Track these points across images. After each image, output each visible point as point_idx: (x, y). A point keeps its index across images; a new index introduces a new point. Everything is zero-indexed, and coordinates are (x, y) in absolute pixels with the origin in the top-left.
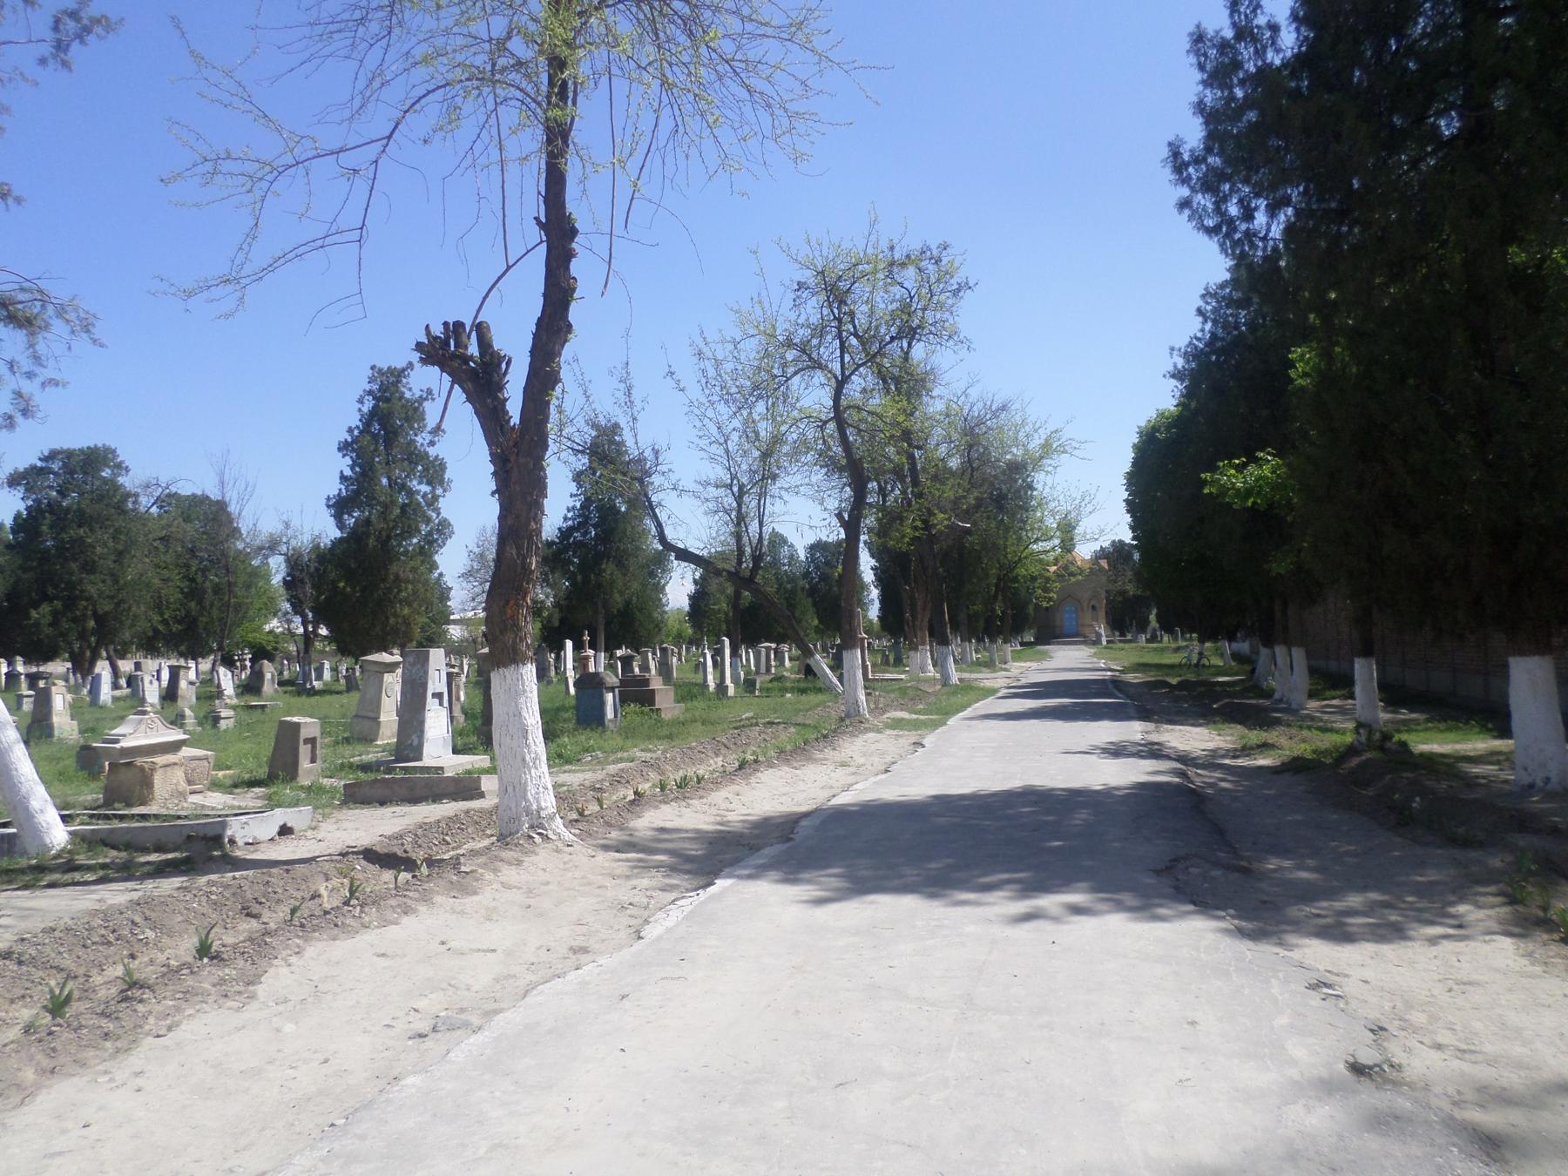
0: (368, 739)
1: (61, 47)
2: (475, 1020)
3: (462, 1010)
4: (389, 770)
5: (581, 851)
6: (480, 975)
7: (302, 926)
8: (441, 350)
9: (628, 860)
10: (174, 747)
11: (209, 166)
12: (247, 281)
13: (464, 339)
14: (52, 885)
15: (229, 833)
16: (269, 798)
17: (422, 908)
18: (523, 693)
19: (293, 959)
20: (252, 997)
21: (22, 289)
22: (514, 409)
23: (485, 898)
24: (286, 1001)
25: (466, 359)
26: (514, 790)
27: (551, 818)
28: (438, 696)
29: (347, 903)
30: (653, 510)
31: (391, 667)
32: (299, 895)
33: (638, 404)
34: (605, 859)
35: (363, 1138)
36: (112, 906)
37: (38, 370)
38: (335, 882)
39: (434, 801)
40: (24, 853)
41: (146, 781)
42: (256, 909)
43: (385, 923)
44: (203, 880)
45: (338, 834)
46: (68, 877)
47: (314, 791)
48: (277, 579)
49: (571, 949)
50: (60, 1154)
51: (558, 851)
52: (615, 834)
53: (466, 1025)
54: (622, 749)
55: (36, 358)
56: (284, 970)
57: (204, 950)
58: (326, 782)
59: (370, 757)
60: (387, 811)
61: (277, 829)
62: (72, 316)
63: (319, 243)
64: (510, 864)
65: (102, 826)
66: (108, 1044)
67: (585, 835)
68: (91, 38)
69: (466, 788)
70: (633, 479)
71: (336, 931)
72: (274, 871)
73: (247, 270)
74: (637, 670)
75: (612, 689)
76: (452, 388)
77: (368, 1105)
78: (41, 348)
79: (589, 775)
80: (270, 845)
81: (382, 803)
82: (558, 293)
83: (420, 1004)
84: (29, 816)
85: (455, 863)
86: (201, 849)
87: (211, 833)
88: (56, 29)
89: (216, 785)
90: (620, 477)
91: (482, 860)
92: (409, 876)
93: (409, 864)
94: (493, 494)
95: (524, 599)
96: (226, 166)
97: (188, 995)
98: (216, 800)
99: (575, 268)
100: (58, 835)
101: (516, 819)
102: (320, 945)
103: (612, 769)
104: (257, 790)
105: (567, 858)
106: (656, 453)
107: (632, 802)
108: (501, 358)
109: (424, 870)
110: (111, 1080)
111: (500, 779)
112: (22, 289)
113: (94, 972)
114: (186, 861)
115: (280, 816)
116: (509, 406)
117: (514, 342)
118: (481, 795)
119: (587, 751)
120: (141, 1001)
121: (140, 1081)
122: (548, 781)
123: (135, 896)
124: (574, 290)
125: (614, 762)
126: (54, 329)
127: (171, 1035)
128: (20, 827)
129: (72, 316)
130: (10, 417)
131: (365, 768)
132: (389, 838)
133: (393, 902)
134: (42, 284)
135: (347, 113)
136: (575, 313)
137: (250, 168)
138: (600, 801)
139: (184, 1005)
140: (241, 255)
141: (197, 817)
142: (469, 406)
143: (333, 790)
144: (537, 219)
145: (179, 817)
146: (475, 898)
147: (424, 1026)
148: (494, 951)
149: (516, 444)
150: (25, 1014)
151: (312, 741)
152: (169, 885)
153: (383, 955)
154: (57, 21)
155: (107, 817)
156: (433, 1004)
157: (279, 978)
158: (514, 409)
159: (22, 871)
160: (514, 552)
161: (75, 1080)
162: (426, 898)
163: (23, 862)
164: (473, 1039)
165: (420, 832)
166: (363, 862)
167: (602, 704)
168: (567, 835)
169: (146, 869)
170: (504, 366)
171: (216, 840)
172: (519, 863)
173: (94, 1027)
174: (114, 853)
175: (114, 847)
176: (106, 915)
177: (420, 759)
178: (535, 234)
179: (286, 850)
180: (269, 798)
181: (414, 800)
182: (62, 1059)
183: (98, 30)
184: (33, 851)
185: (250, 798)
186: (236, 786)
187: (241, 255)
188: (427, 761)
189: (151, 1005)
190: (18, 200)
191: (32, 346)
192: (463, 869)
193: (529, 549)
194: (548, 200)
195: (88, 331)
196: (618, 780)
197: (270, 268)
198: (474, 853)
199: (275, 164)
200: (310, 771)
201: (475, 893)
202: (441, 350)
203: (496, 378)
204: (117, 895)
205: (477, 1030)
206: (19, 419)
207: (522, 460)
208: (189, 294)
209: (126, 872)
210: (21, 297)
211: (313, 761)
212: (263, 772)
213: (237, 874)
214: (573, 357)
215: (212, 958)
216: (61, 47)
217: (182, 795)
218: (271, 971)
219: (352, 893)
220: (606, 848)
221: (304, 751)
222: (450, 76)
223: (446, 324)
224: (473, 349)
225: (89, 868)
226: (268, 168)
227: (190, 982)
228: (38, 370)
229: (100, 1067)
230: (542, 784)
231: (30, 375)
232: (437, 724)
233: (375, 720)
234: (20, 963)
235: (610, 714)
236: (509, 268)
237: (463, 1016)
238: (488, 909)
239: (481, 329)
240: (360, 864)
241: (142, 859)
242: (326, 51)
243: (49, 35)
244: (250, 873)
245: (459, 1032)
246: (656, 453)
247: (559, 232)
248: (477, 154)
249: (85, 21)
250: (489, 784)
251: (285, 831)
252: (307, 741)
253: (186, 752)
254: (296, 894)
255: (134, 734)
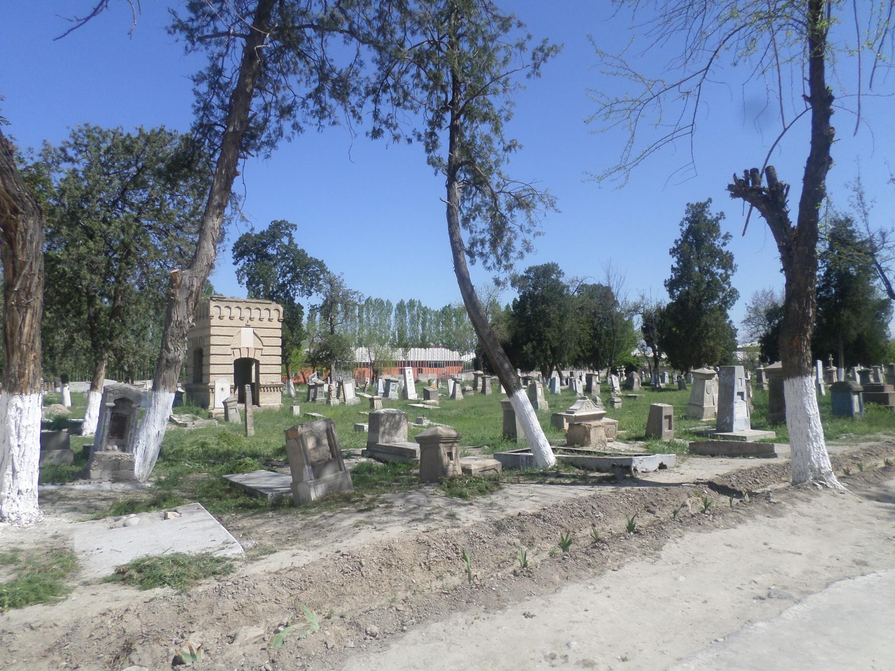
0: (698, 417)
1: (536, 66)
2: (796, 596)
3: (785, 588)
4: (715, 437)
5: (851, 498)
6: (794, 568)
7: (681, 521)
8: (744, 188)
9: (886, 507)
10: (599, 417)
11: (607, 109)
12: (630, 166)
13: (758, 177)
14: (552, 483)
15: (634, 465)
16: (647, 447)
17: (749, 521)
18: (808, 392)
19: (678, 540)
20: (659, 557)
21: (524, 190)
22: (793, 217)
23: (788, 519)
24: (677, 563)
25: (760, 190)
26: (802, 454)
27: (829, 474)
28: (741, 394)
29: (703, 512)
30: (882, 273)
31: (710, 377)
32: (675, 503)
33: (868, 204)
34: (870, 505)
35: (737, 653)
36: (581, 497)
37: (532, 228)
38: (694, 499)
39: (744, 457)
40: (537, 466)
41: (587, 434)
42: (652, 508)
43: (728, 527)
44: (623, 489)
45: (691, 471)
46: (558, 480)
47: (672, 447)
48: (655, 330)
49: (854, 561)
50: (577, 622)
51: (834, 495)
52: (874, 489)
53: (790, 597)
54: (869, 432)
55: (531, 222)
56: (674, 545)
57: (631, 528)
58: (677, 440)
59: (701, 428)
60: (717, 460)
61: (658, 465)
62: (546, 200)
63: (670, 138)
64: (803, 501)
65: (570, 455)
66: (590, 570)
67: (852, 487)
68: (549, 59)
69: (763, 450)
70: (866, 253)
71: (700, 527)
72: (660, 488)
73: (630, 160)
74: (872, 380)
75: (857, 393)
76: (751, 209)
77: (737, 633)
78: (533, 217)
79: (847, 448)
80: (655, 474)
81: (713, 456)
82: (822, 139)
83: (758, 579)
84: (539, 448)
85: (767, 496)
86: (620, 473)
87: (624, 464)
88: (534, 58)
89: (619, 438)
90: (856, 253)
91: (784, 496)
92: (737, 501)
93: (739, 494)
94: (781, 271)
95: (805, 335)
96: (617, 107)
97: (626, 550)
98: (621, 446)
99: (833, 121)
100: (551, 459)
101: (804, 473)
102: (693, 534)
103: (864, 445)
104: (640, 442)
105: (842, 501)
106: (883, 235)
107: (884, 469)
108: (783, 187)
109: (747, 498)
110: (595, 588)
111: (792, 447)
112: (524, 190)
113: (577, 530)
114: (613, 478)
115: (659, 458)
116: (790, 216)
117: (792, 175)
118: (775, 456)
119: (842, 432)
120: (603, 549)
121: (608, 592)
122: (825, 450)
123: (592, 493)
124: (833, 135)
125: (864, 441)
126: (537, 207)
127: (620, 571)
128: (535, 453)
129: (546, 200)
130: (521, 253)
131: (699, 434)
132: (722, 476)
133: (731, 515)
134: (533, 186)
135: (682, 61)
136: (834, 151)
137: (628, 105)
138: (860, 467)
139: (624, 555)
140: (626, 154)
141: (616, 455)
142: (763, 219)
143: (682, 447)
144: (804, 96)
145: (606, 454)
146: (781, 519)
147: (763, 593)
148: (800, 554)
149: (795, 239)
150: (549, 546)
151: (669, 417)
152: (607, 490)
153: (730, 545)
154: (534, 54)
155: (572, 451)
156: (765, 580)
157: (672, 549)
158: (793, 217)
159: (538, 475)
160: (797, 306)
161: (578, 585)
162: (750, 515)
163: (537, 471)
164: (796, 607)
165: (740, 475)
166: (708, 489)
167: (850, 402)
168: (840, 486)
169: (594, 480)
170: (785, 191)
171: (627, 468)
172: (809, 501)
173: (582, 560)
174: (577, 470)
175: (577, 467)
176: (580, 501)
177: (732, 431)
178: (802, 105)
179: (663, 478)
180: (647, 447)
181: (732, 455)
182: (571, 573)
183: (552, 53)
184: (541, 466)
185: (638, 447)
186: (629, 440)
187: (626, 154)
188: (736, 432)
189: (610, 553)
190: (520, 147)
191: (529, 217)
192: (772, 500)
193: (807, 302)
194: (812, 82)
195: (553, 206)
196: (870, 453)
197: (642, 157)
198: (777, 491)
199: (642, 99)
200: (668, 434)
201: (781, 516)
202: (744, 188)
203: (780, 200)
204: (583, 492)
205: (798, 602)
206: (525, 253)
207: (800, 248)
208: (600, 179)
209: (584, 481)
210: (524, 194)
211: (670, 428)
212: (643, 433)
213: (641, 488)
214: (832, 181)
215: (635, 533)
216: (536, 66)
217: (604, 442)
218: (667, 544)
219: (706, 506)
220: (869, 497)
221: (665, 422)
222: (748, 21)
223: (746, 171)
224: (764, 184)
225: (567, 477)
226: (638, 103)
227: (626, 543)
228: (532, 228)
229: (588, 581)
230: (821, 453)
231: (529, 231)
232: (741, 411)
233: (701, 407)
234: (544, 521)
235: (856, 409)
236: (785, 130)
237: (786, 591)
238: (791, 527)
239: (769, 172)
240: (707, 490)
241: (592, 475)
242: (672, 28)
243: (531, 62)
244: (647, 488)
245: (786, 601)
246: (883, 235)
247: (820, 101)
248: (765, 65)
249: (546, 51)
250: (779, 448)
251: (662, 467)
252: (666, 417)
253: (605, 420)
254: (673, 503)
255: (582, 409)
